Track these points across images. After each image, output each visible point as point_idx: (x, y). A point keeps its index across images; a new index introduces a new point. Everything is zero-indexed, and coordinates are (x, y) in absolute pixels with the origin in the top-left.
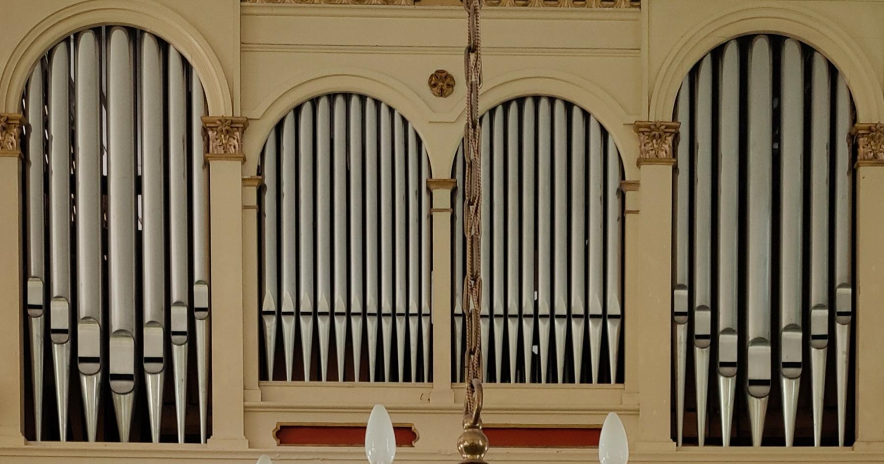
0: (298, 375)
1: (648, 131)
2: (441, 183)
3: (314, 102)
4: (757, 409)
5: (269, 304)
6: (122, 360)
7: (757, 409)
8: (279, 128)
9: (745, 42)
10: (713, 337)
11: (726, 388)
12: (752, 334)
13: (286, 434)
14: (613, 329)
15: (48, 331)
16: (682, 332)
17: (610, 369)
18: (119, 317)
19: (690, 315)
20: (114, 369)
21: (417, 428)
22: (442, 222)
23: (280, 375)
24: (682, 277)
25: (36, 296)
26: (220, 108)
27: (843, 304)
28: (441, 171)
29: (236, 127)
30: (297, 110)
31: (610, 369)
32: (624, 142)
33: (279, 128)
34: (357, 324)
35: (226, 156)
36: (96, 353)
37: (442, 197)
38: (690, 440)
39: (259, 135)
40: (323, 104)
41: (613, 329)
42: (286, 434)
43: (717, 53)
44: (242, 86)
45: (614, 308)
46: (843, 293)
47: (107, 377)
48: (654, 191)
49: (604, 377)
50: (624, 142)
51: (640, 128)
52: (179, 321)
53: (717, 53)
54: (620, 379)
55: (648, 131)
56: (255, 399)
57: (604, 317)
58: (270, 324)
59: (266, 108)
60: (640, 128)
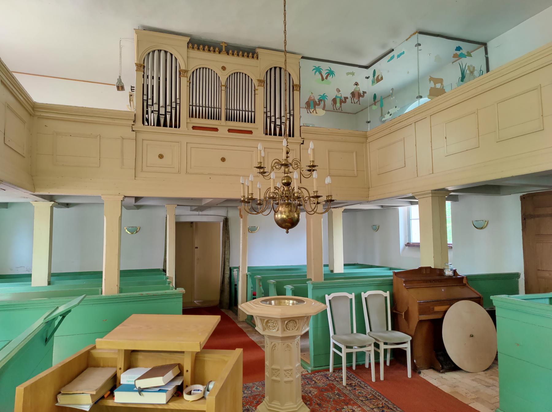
0: (196, 117)
1: (260, 81)
2: (223, 86)
3: (200, 68)
4: (278, 130)
5: (191, 104)
7: (278, 130)
8: (193, 72)
9: (275, 68)
10: (270, 117)
12: (277, 117)
13: (194, 128)
14: (253, 114)
15: (147, 105)
16: (265, 115)
17: (252, 121)
18: (162, 103)
19: (267, 112)
20: (161, 113)
21: (219, 128)
22: (223, 93)
23: (192, 117)
24: (265, 106)
25: (145, 98)
26: (183, 67)
27: (292, 113)
28: (223, 83)
29: (186, 71)
30: (197, 70)
31: (252, 121)
32: (255, 82)
33: (193, 72)
34: (207, 109)
37: (223, 88)
38: (266, 134)
39: (190, 73)
40: (201, 69)
41: (253, 114)
42: (194, 128)
43: (271, 69)
44: (187, 64)
45: (253, 110)
46: (292, 112)
48: (261, 91)
49: (251, 122)
50: (255, 82)
53: (271, 69)
54: (254, 122)
55: (260, 81)
56: (189, 121)
57: (251, 111)
58: (191, 107)
59: (191, 69)
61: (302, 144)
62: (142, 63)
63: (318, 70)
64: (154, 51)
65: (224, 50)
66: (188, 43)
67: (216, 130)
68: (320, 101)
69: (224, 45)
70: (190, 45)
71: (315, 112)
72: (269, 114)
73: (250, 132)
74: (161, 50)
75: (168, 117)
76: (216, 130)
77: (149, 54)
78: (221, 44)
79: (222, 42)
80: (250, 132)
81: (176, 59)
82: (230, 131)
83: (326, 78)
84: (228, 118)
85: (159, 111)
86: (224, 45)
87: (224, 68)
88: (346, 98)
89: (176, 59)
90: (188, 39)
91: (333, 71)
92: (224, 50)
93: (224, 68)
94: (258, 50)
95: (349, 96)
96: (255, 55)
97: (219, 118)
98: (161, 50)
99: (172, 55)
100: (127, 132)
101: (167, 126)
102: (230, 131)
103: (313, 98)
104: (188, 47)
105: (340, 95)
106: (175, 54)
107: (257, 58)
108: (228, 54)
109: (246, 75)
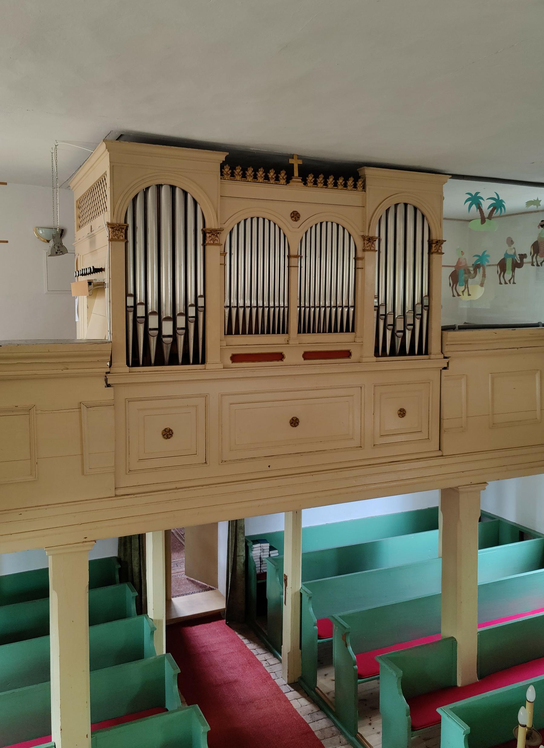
4: (398, 342)
6: (167, 328)
7: (398, 342)
9: (396, 205)
10: (386, 315)
11: (389, 334)
21: (285, 353)
29: (216, 232)
31: (348, 326)
35: (213, 244)
36: (157, 326)
47: (160, 337)
49: (347, 331)
51: (363, 237)
52: (192, 312)
54: (353, 331)
60: (363, 237)
61: (445, 368)
62: (123, 221)
63: (475, 200)
64: (147, 189)
65: (296, 173)
66: (222, 166)
67: (280, 357)
68: (477, 267)
69: (296, 163)
70: (227, 169)
71: (466, 293)
72: (382, 312)
73: (347, 354)
74: (162, 185)
75: (181, 340)
76: (280, 357)
77: (136, 196)
78: (291, 161)
79: (292, 156)
80: (347, 354)
81: (195, 203)
82: (307, 356)
83: (490, 217)
84: (305, 328)
85: (160, 329)
86: (296, 163)
87: (295, 216)
88: (522, 256)
89: (195, 203)
90: (221, 157)
91: (502, 201)
92: (296, 173)
93: (295, 216)
94: (369, 172)
95: (527, 249)
96: (360, 183)
97: (284, 330)
98: (162, 185)
99: (185, 193)
100: (96, 391)
101: (177, 363)
102: (307, 356)
103: (463, 264)
104: (222, 175)
105: (511, 252)
106: (194, 192)
107: (364, 188)
108: (305, 184)
109: (338, 225)
